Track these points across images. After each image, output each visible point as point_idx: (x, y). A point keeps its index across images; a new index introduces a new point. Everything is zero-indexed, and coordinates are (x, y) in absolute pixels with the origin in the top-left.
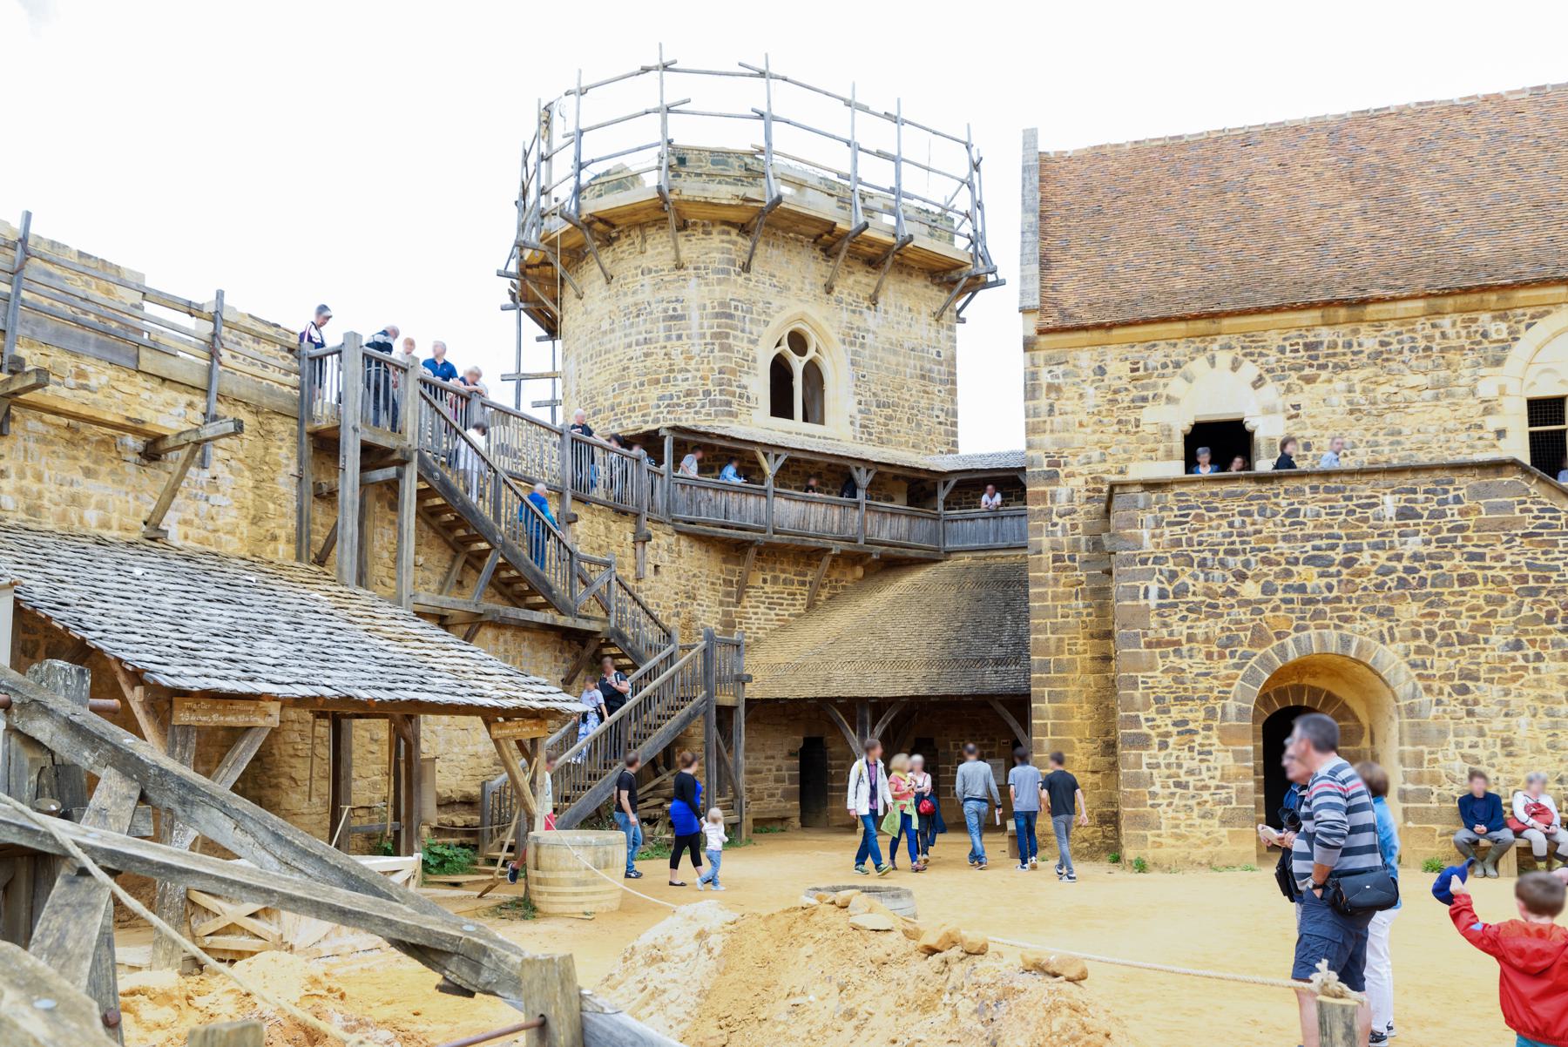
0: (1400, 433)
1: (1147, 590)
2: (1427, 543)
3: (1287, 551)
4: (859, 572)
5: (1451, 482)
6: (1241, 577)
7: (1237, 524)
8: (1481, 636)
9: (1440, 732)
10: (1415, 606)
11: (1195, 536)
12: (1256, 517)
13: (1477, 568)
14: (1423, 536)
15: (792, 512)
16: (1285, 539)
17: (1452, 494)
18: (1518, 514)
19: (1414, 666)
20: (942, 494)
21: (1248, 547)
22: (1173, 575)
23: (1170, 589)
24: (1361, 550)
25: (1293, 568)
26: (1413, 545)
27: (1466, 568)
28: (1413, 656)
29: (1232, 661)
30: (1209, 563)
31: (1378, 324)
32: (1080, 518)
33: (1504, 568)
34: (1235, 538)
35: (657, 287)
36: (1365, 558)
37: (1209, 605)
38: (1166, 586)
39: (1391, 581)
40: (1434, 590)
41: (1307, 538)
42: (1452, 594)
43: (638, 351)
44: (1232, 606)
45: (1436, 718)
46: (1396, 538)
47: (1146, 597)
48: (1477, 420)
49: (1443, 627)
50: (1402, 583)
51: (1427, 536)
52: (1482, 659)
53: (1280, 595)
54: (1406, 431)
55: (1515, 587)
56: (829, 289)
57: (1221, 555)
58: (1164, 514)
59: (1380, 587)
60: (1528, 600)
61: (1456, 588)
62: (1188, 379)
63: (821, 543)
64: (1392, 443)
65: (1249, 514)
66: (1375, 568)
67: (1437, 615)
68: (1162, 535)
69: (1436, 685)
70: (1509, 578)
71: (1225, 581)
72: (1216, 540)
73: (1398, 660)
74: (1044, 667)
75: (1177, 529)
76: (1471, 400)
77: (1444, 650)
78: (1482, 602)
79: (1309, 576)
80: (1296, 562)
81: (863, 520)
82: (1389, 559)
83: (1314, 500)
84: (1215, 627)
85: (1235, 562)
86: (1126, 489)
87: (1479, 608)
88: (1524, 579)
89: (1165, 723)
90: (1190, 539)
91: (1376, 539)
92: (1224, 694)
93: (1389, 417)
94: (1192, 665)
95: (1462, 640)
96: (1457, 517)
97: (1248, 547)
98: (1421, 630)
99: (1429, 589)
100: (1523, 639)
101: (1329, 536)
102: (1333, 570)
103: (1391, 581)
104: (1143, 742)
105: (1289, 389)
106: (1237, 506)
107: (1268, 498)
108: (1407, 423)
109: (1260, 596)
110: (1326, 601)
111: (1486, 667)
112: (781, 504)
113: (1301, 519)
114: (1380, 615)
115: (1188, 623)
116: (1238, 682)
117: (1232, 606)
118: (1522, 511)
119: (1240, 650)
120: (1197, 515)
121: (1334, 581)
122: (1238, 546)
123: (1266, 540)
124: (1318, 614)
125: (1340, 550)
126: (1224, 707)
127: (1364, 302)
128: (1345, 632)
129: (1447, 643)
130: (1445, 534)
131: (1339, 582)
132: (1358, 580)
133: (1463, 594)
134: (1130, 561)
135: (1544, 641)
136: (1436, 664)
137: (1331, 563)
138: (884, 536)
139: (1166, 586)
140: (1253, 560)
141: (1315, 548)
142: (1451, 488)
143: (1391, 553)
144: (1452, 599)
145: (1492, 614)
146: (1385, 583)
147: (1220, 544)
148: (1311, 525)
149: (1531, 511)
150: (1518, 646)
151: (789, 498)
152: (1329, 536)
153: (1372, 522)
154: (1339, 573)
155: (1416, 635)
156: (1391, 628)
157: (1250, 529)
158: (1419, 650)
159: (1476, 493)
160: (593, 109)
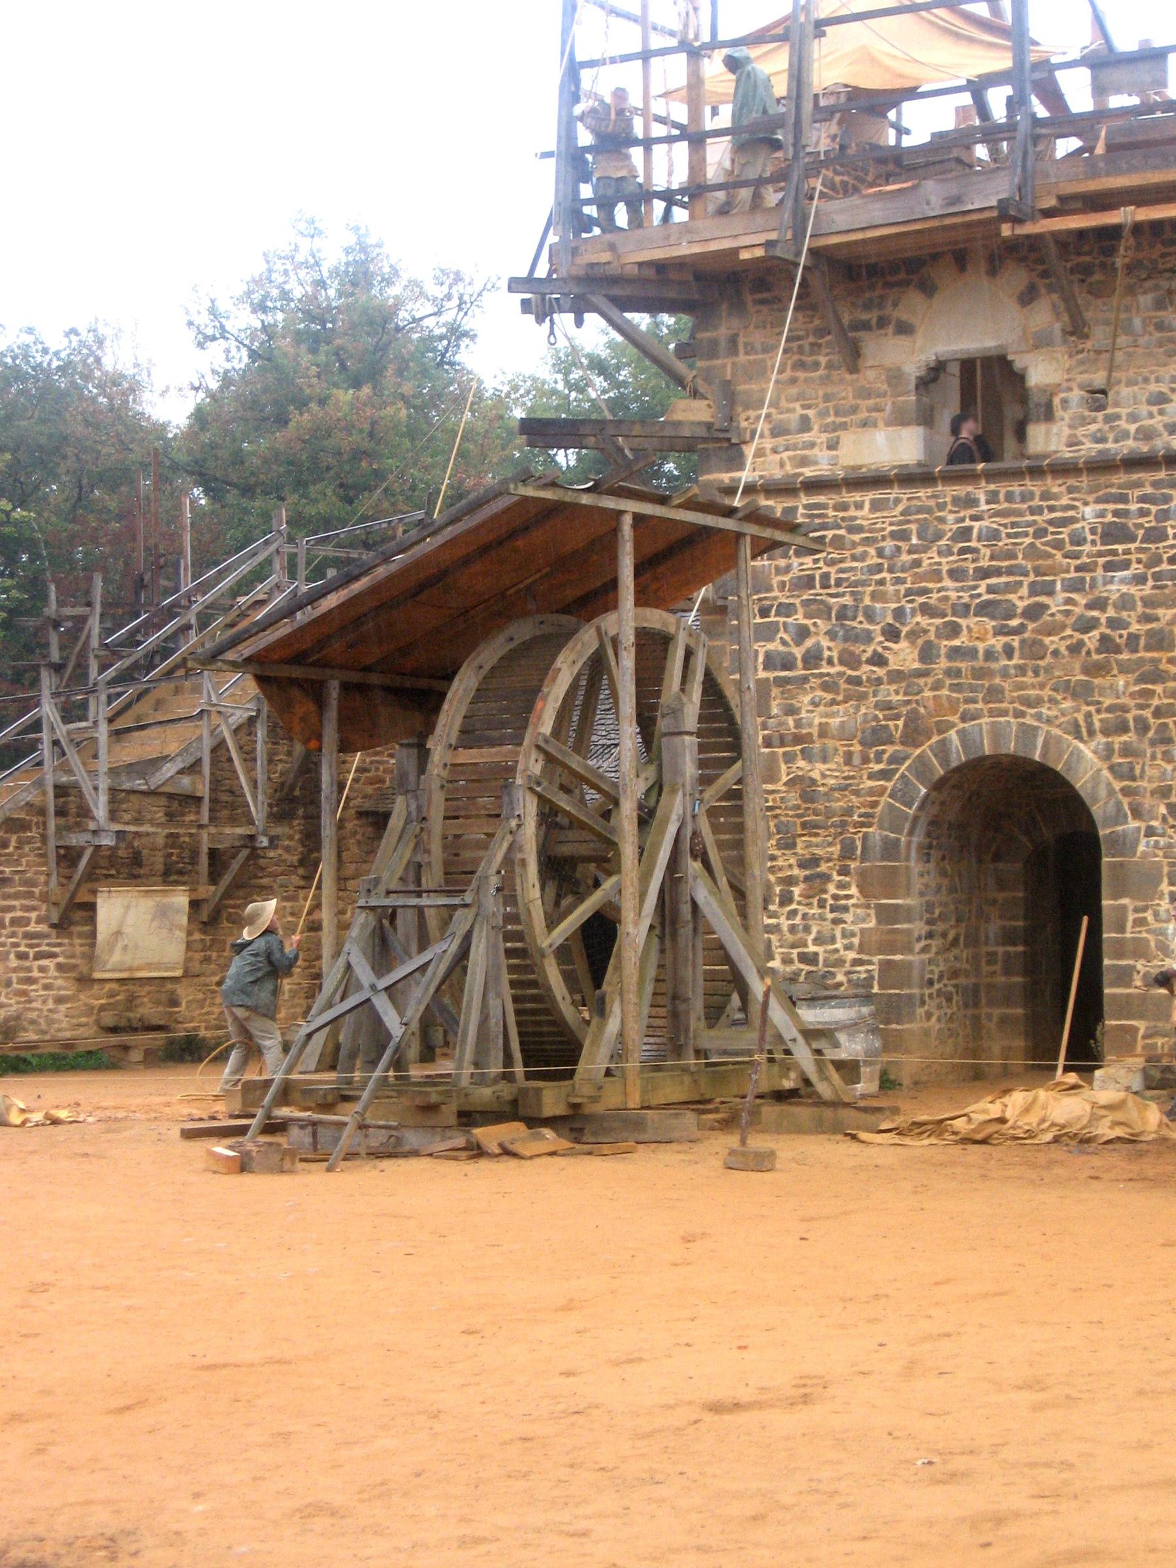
2: (1140, 580)
3: (953, 595)
6: (892, 634)
7: (887, 552)
11: (832, 570)
14: (1135, 569)
16: (955, 574)
21: (902, 588)
25: (963, 622)
28: (1117, 760)
29: (878, 767)
36: (1055, 604)
39: (1091, 640)
40: (1149, 655)
41: (984, 574)
44: (879, 681)
46: (1100, 572)
49: (1157, 713)
50: (1106, 644)
57: (867, 601)
59: (1076, 648)
65: (903, 536)
66: (1072, 620)
67: (1151, 693)
69: (1147, 802)
73: (1099, 764)
75: (808, 561)
77: (1160, 750)
82: (1089, 606)
90: (826, 576)
91: (1073, 575)
98: (1130, 716)
101: (1010, 571)
102: (1014, 623)
103: (1091, 640)
109: (916, 665)
110: (1005, 674)
113: (973, 544)
114: (1075, 696)
116: (885, 799)
128: (1029, 721)
132: (1047, 640)
141: (991, 590)
146: (1081, 644)
155: (1123, 728)
157: (905, 557)
158: (1126, 750)
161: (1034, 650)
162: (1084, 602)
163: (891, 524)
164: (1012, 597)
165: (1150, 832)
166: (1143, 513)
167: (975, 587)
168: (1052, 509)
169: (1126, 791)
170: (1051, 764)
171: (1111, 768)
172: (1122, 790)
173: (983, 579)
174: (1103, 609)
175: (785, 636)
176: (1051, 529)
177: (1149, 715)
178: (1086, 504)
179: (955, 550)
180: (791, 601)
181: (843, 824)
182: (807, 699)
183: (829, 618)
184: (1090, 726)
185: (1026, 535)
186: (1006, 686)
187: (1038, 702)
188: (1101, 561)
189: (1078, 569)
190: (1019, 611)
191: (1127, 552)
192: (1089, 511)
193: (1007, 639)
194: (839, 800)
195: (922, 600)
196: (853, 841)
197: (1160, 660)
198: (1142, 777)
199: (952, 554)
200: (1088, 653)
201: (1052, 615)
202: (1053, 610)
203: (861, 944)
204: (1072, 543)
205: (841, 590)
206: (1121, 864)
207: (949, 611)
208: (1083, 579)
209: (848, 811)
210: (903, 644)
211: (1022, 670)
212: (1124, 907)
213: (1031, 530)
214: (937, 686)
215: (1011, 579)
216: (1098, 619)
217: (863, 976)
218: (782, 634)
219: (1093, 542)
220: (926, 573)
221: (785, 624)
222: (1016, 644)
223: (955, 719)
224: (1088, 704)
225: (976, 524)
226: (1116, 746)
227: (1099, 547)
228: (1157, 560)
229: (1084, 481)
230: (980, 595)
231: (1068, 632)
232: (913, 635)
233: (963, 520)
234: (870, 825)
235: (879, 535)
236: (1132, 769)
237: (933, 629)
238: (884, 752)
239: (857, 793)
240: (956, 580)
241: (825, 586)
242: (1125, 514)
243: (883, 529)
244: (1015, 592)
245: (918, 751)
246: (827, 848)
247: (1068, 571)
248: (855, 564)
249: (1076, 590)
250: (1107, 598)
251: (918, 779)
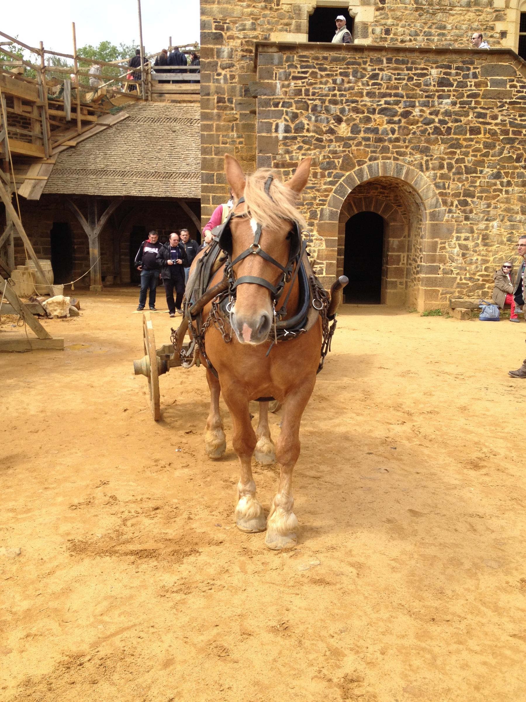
0: (444, 28)
1: (277, 126)
3: (369, 104)
5: (472, 63)
6: (339, 120)
7: (338, 82)
8: (479, 169)
9: (448, 230)
10: (442, 147)
12: (351, 78)
13: (481, 123)
16: (369, 94)
17: (472, 71)
18: (508, 88)
19: (437, 186)
21: (344, 99)
22: (295, 116)
23: (292, 126)
24: (414, 106)
26: (446, 104)
28: (438, 180)
29: (329, 179)
30: (319, 109)
33: (496, 125)
34: (336, 92)
36: (416, 112)
37: (318, 140)
38: (290, 124)
39: (430, 128)
41: (384, 95)
42: (465, 140)
44: (331, 141)
45: (447, 221)
46: (436, 99)
47: (276, 130)
48: (491, 23)
49: (457, 161)
51: (455, 99)
52: (478, 184)
53: (362, 135)
54: (449, 27)
55: (501, 137)
57: (327, 103)
58: (292, 70)
59: (424, 132)
60: (508, 146)
61: (468, 136)
64: (439, 35)
65: (346, 75)
66: (421, 119)
67: (455, 153)
68: (289, 86)
69: (449, 200)
70: (498, 131)
71: (328, 122)
72: (325, 92)
75: (300, 82)
76: (488, 10)
78: (481, 146)
80: (374, 112)
82: (431, 114)
83: (389, 68)
85: (335, 109)
86: (266, 49)
87: (478, 150)
88: (506, 132)
90: (307, 91)
91: (424, 99)
92: (323, 202)
93: (439, 16)
95: (468, 171)
96: (473, 88)
97: (344, 99)
99: (452, 136)
100: (502, 171)
101: (396, 95)
102: (396, 119)
103: (430, 128)
106: (339, 69)
107: (359, 64)
108: (450, 22)
109: (349, 134)
110: (390, 141)
111: (479, 189)
113: (379, 81)
115: (303, 152)
116: (332, 194)
117: (331, 141)
118: (511, 86)
119: (335, 172)
120: (313, 73)
121: (396, 127)
122: (338, 98)
123: (356, 95)
125: (401, 105)
126: (322, 210)
129: (459, 173)
130: (465, 99)
131: (399, 128)
132: (411, 127)
133: (471, 140)
134: (266, 103)
135: (513, 173)
136: (451, 186)
137: (395, 114)
139: (290, 124)
140: (347, 108)
141: (386, 103)
142: (472, 67)
143: (432, 109)
144: (465, 143)
145: (486, 155)
146: (426, 130)
147: (327, 95)
148: (385, 85)
149: (515, 87)
150: (498, 176)
152: (396, 95)
153: (423, 87)
154: (400, 121)
155: (441, 167)
156: (427, 161)
157: (347, 86)
158: (442, 177)
159: (487, 72)
161: (405, 131)
162: (428, 111)
163: (340, 68)
164: (396, 107)
165: (450, 211)
166: (457, 74)
167: (379, 101)
168: (416, 69)
169: (441, 194)
170: (409, 181)
171: (435, 184)
172: (439, 193)
173: (382, 97)
174: (437, 115)
175: (287, 118)
176: (415, 78)
177: (454, 162)
178: (432, 68)
179: (370, 84)
180: (289, 101)
181: (312, 204)
182: (296, 147)
183: (308, 110)
184: (427, 165)
185: (404, 79)
186: (391, 147)
187: (403, 154)
188: (437, 94)
189: (427, 97)
190: (399, 113)
191: (449, 91)
192: (434, 72)
193: (393, 126)
194: (309, 193)
195: (354, 105)
196: (316, 211)
197: (460, 139)
198: (448, 188)
199: (368, 85)
200: (429, 134)
201: (414, 116)
202: (414, 114)
203: (318, 256)
204: (424, 85)
205: (314, 97)
206: (437, 224)
207: (366, 111)
208: (429, 101)
209: (315, 198)
210: (343, 125)
211: (397, 140)
212: (437, 242)
213: (406, 77)
214: (359, 144)
215: (396, 98)
216: (434, 120)
217: (318, 269)
218: (284, 116)
219: (434, 86)
220: (356, 93)
221: (286, 112)
222: (397, 128)
223: (367, 160)
224: (427, 156)
225: (381, 73)
226: (438, 175)
227: (436, 88)
228: (463, 96)
229: (432, 57)
230: (381, 105)
231: (420, 124)
232: (347, 121)
233: (375, 70)
234: (324, 205)
235: (334, 73)
236: (444, 185)
237: (358, 119)
238: (332, 172)
239: (318, 191)
240: (370, 97)
241: (307, 95)
242: (449, 74)
243: (337, 71)
244: (398, 105)
245: (347, 174)
247: (422, 98)
248: (322, 86)
249: (425, 106)
250: (439, 111)
251: (348, 185)
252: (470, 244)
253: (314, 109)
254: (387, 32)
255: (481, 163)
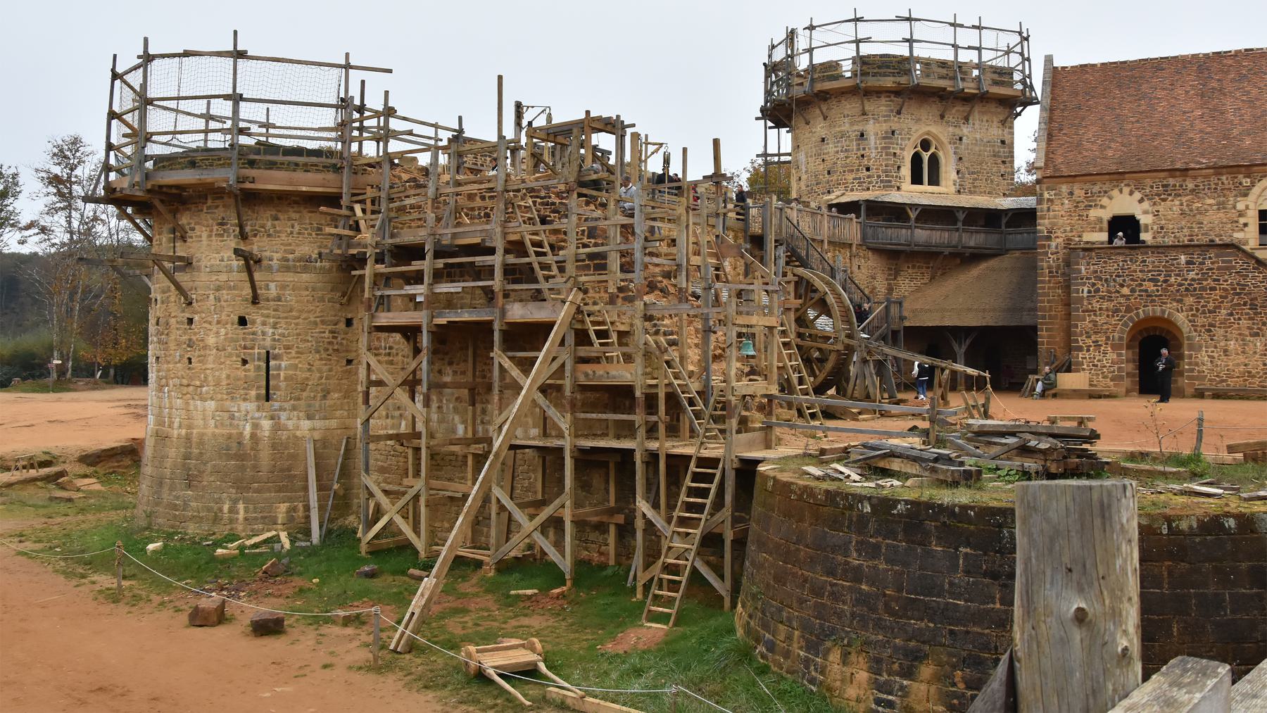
4: (958, 261)
6: (1122, 286)
15: (922, 235)
20: (1004, 221)
26: (1192, 275)
27: (1213, 284)
31: (1195, 178)
32: (1061, 256)
35: (852, 124)
36: (1172, 280)
39: (1183, 289)
43: (842, 155)
50: (1187, 289)
56: (942, 117)
62: (1111, 198)
63: (938, 250)
74: (1044, 317)
79: (1150, 286)
81: (960, 237)
84: (1111, 305)
89: (1089, 342)
94: (1101, 320)
95: (1210, 312)
103: (1183, 289)
104: (1080, 349)
105: (1155, 204)
112: (918, 232)
124: (1153, 301)
127: (1187, 170)
129: (1204, 312)
138: (972, 244)
150: (1231, 314)
151: (922, 228)
159: (1217, 256)
160: (819, 37)
246: (1102, 339)
252: (1215, 355)
253: (1106, 280)
254: (1162, 228)
255: (1219, 307)
